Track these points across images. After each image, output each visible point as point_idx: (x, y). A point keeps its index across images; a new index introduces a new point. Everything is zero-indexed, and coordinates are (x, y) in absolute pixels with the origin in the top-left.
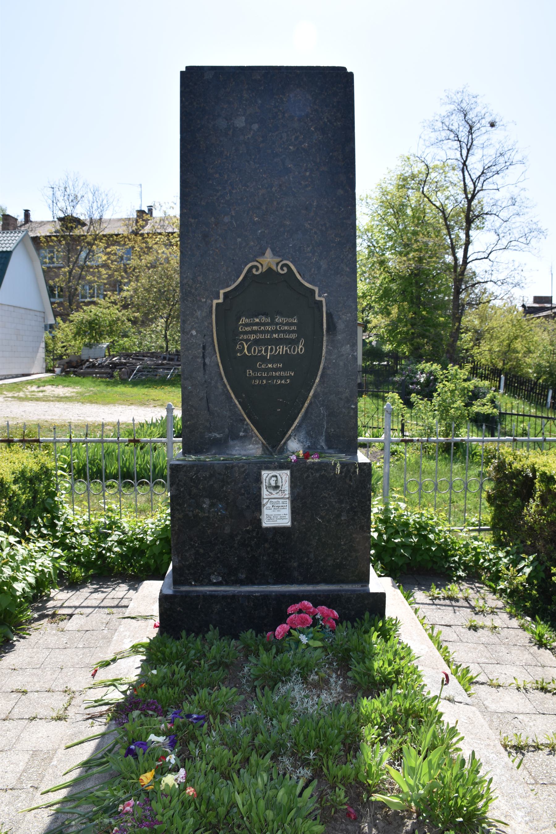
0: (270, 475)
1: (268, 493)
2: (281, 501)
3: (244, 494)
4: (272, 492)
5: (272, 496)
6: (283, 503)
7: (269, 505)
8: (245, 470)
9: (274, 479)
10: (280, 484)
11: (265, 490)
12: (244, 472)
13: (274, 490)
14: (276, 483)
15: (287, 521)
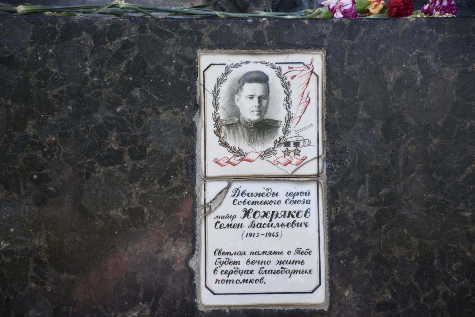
0: (237, 73)
1: (224, 153)
2: (282, 189)
3: (116, 158)
4: (244, 146)
5: (244, 169)
6: (292, 198)
7: (227, 207)
8: (126, 45)
9: (255, 89)
10: (278, 113)
11: (212, 139)
12: (118, 57)
13: (251, 141)
14: (262, 110)
15: (309, 281)
